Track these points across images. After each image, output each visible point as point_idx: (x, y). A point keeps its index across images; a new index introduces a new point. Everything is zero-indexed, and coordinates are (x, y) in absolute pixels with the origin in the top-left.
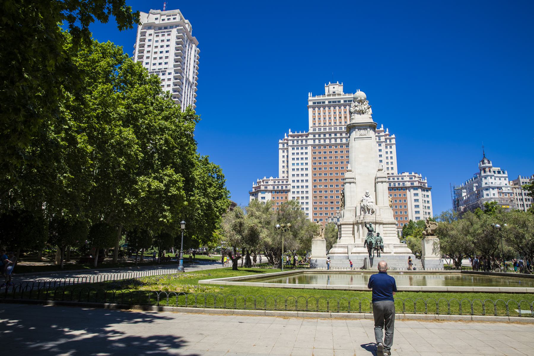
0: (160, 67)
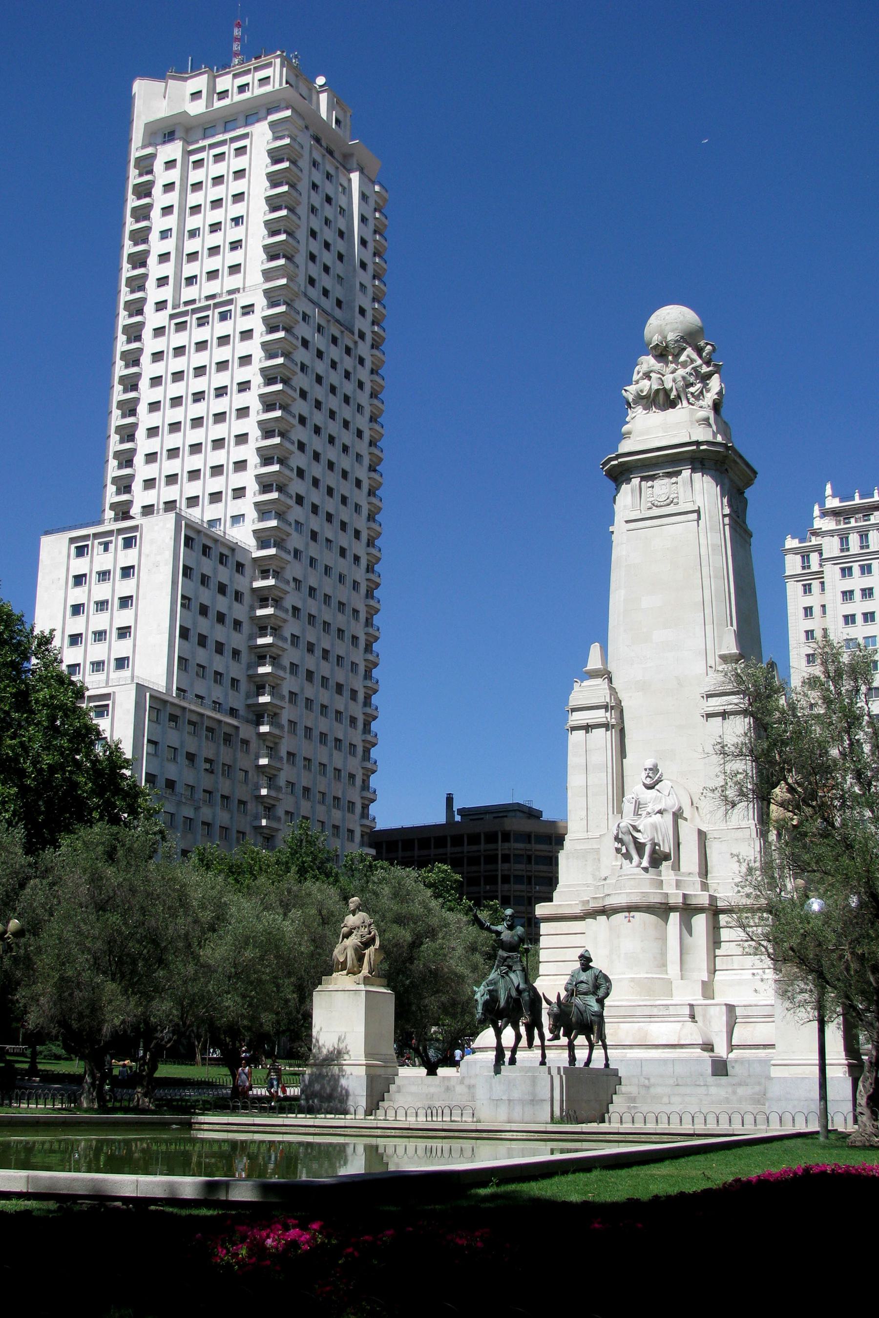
0: (213, 287)
